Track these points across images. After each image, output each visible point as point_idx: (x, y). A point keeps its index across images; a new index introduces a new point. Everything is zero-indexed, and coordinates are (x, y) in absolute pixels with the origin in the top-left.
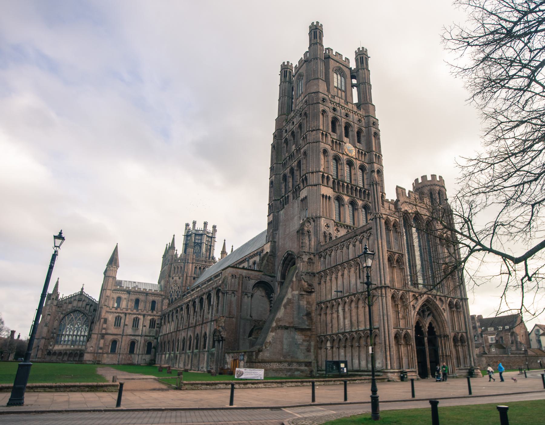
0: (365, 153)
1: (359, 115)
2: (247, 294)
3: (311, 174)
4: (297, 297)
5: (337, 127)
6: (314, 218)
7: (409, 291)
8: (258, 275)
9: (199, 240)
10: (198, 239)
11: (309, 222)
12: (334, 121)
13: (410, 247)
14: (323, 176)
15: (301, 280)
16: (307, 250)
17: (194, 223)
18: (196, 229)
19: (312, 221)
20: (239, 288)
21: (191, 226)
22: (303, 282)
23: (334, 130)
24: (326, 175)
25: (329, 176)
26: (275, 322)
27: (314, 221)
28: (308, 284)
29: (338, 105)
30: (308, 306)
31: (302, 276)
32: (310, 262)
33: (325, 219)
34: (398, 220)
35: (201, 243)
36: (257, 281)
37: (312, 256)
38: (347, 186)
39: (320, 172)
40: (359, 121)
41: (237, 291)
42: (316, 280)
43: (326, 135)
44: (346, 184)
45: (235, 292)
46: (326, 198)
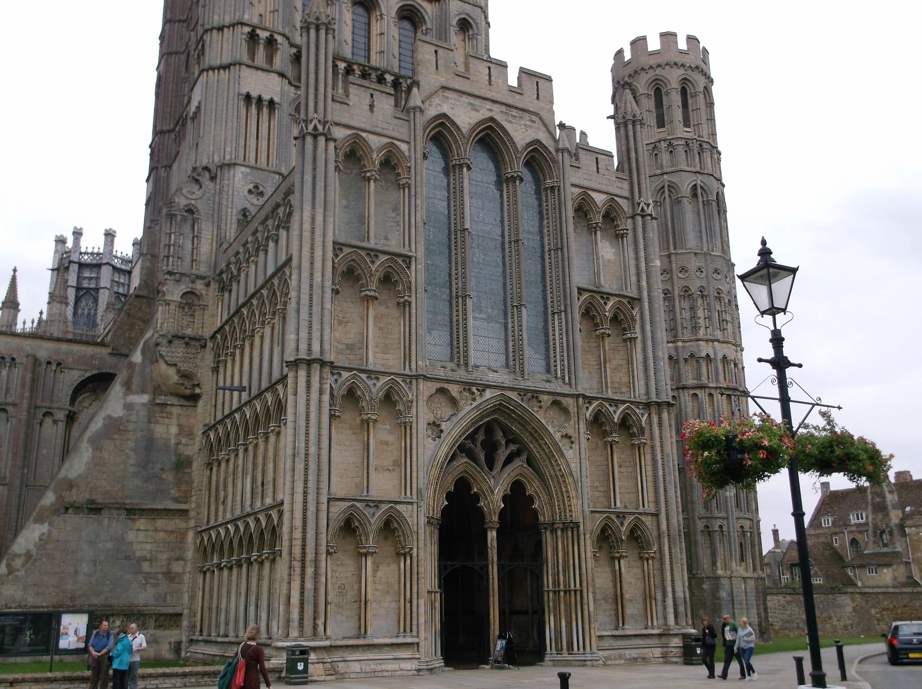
2: (51, 414)
3: (215, 32)
4: (143, 413)
6: (213, 168)
7: (417, 377)
8: (92, 357)
9: (93, 281)
10: (90, 279)
11: (197, 181)
13: (453, 237)
14: (253, 37)
15: (157, 361)
16: (184, 266)
17: (78, 234)
18: (83, 250)
19: (205, 178)
20: (22, 396)
21: (70, 244)
22: (163, 367)
24: (263, 34)
25: (276, 36)
26: (55, 491)
27: (213, 178)
28: (179, 371)
30: (184, 441)
31: (159, 348)
32: (190, 305)
33: (248, 170)
34: (404, 147)
35: (97, 290)
36: (88, 375)
37: (199, 286)
39: (243, 24)
41: (15, 405)
42: (208, 357)
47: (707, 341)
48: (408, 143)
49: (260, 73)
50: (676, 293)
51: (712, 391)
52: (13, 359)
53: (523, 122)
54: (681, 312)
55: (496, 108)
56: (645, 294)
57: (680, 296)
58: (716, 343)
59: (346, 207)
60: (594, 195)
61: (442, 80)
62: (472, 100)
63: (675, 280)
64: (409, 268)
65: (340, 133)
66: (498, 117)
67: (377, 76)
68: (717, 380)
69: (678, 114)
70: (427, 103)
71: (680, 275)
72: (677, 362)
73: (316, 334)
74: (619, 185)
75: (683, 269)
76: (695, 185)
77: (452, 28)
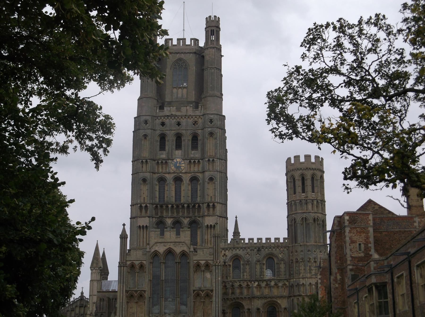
0: (199, 161)
1: (194, 117)
5: (167, 143)
12: (163, 137)
14: (141, 206)
23: (162, 147)
24: (144, 205)
25: (148, 205)
29: (166, 118)
34: (145, 262)
38: (172, 207)
39: (137, 204)
40: (195, 123)
43: (147, 161)
44: (170, 206)
45: (104, 314)
46: (143, 229)
47: (303, 278)
48: (146, 261)
49: (143, 218)
50: (294, 260)
51: (304, 297)
52: (103, 299)
53: (179, 246)
54: (295, 268)
55: (172, 244)
56: (214, 289)
57: (295, 262)
58: (306, 279)
59: (133, 279)
60: (201, 262)
61: (156, 241)
62: (164, 244)
63: (294, 256)
64: (145, 293)
65: (128, 263)
66: (172, 247)
67: (182, 206)
68: (306, 293)
69: (299, 189)
70: (151, 249)
71: (296, 254)
72: (293, 286)
73: (121, 314)
74: (210, 257)
75: (297, 252)
76: (303, 218)
77: (206, 183)
